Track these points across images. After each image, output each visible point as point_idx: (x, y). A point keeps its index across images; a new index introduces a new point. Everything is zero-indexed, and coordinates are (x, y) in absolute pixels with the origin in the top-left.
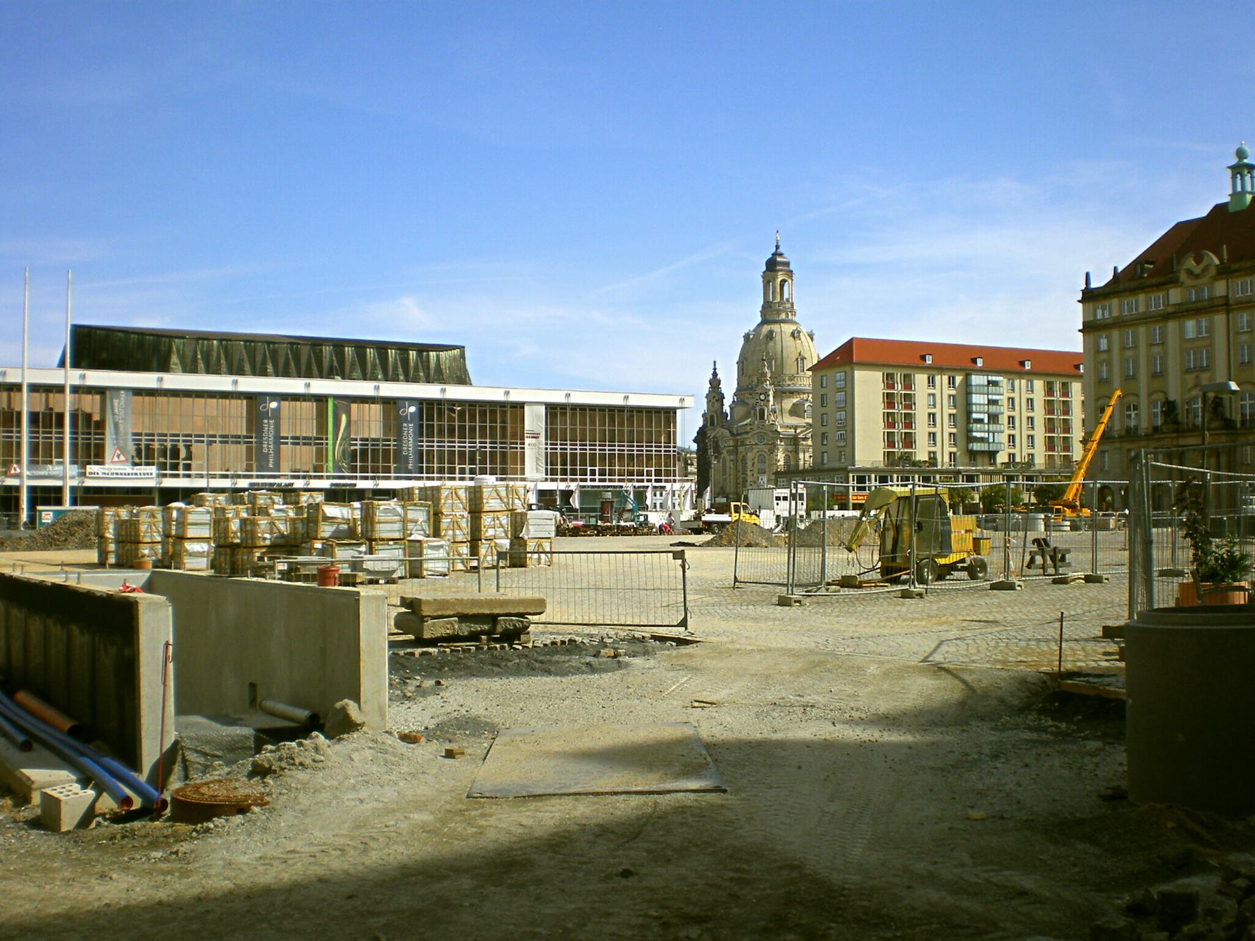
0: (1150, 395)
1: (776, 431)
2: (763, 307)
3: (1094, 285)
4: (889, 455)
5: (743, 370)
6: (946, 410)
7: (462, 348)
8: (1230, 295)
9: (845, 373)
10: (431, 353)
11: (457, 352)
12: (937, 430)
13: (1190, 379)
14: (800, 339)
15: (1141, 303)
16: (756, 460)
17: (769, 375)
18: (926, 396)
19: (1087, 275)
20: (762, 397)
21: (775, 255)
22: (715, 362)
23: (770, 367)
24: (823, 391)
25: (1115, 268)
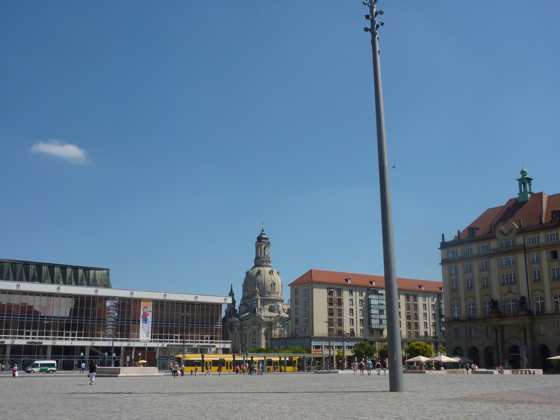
0: (481, 297)
1: (261, 319)
2: (256, 259)
3: (446, 240)
4: (329, 330)
5: (245, 288)
6: (358, 308)
7: (109, 270)
8: (526, 244)
9: (308, 287)
10: (91, 271)
11: (105, 271)
12: (354, 317)
13: (505, 289)
14: (273, 275)
15: (475, 248)
16: (251, 334)
17: (258, 291)
18: (349, 300)
19: (443, 235)
20: (255, 302)
21: (261, 234)
22: (232, 285)
23: (259, 288)
24: (297, 296)
25: (459, 231)
